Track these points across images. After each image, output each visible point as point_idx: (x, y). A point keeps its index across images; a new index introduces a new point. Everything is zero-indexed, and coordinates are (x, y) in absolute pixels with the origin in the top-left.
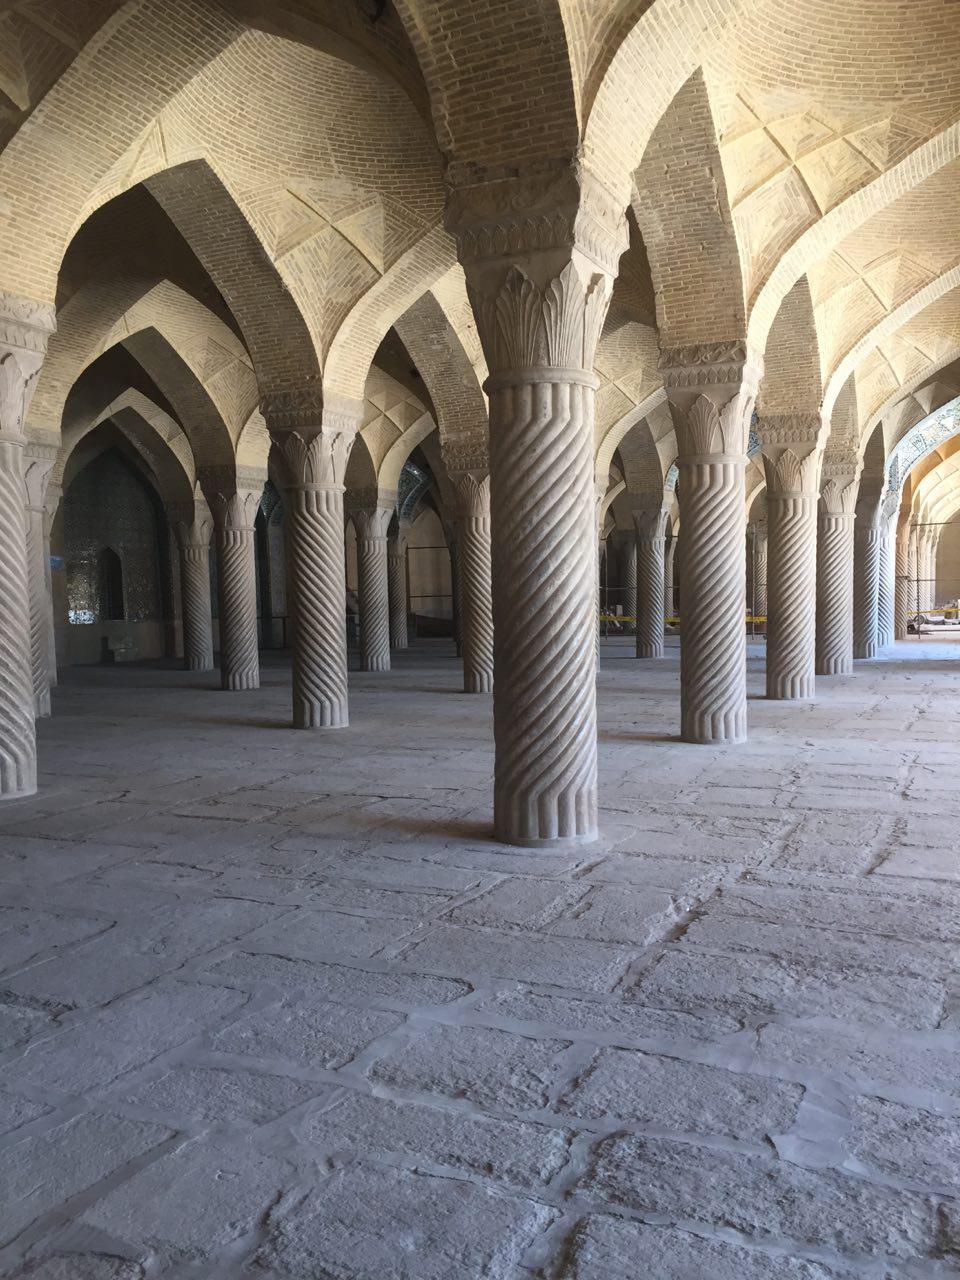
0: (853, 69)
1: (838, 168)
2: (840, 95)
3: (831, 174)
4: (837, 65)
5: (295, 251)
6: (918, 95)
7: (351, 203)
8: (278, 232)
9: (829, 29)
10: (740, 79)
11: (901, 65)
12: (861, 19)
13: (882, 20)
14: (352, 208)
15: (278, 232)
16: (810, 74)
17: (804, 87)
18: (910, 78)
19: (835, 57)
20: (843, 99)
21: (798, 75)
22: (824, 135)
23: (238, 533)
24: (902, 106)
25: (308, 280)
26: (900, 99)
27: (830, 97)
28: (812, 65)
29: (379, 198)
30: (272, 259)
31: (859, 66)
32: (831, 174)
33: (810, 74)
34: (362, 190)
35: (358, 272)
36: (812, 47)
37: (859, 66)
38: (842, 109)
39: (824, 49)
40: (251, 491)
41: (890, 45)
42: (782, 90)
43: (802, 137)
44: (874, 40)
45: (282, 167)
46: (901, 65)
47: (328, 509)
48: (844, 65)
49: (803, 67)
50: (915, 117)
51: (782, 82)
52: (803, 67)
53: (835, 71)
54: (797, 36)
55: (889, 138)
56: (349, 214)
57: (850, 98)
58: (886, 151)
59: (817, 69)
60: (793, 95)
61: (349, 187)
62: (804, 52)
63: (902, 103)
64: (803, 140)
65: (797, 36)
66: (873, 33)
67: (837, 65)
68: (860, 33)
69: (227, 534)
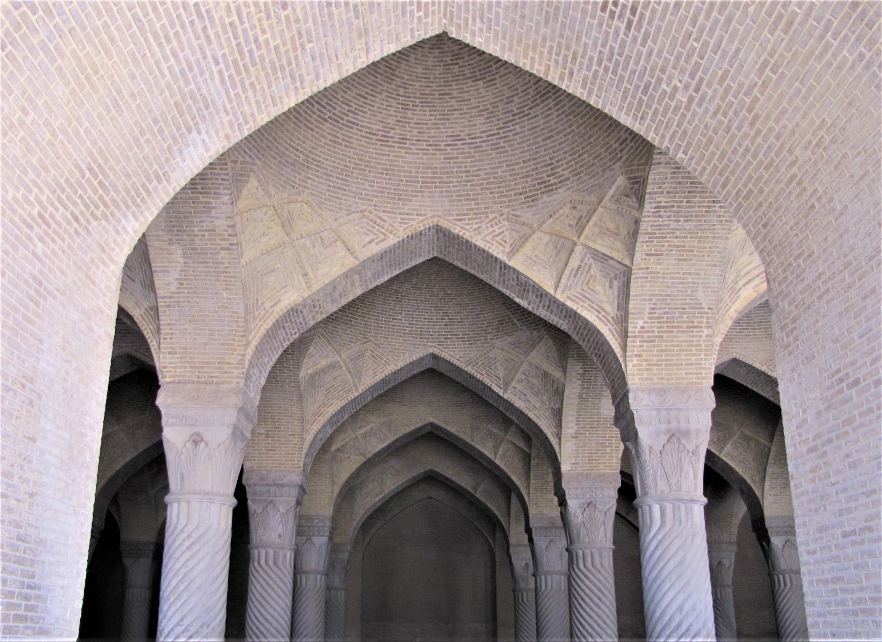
0: (586, 156)
1: (618, 227)
2: (586, 178)
3: (616, 234)
4: (574, 159)
5: (514, 384)
6: (629, 147)
7: (531, 342)
8: (501, 375)
9: (553, 142)
10: (505, 211)
11: (610, 134)
12: (567, 122)
13: (578, 114)
14: (533, 347)
15: (501, 375)
16: (561, 176)
17: (560, 187)
18: (619, 139)
19: (570, 155)
20: (590, 179)
21: (553, 181)
22: (589, 212)
23: (781, 576)
24: (624, 162)
25: (534, 400)
26: (621, 157)
27: (581, 183)
28: (559, 170)
29: (545, 332)
30: (501, 394)
31: (587, 151)
32: (616, 234)
33: (561, 176)
34: (535, 332)
35: (555, 385)
36: (551, 159)
37: (587, 151)
38: (592, 186)
39: (560, 155)
40: (788, 537)
41: (595, 126)
42: (546, 198)
43: (575, 221)
44: (585, 128)
45: (489, 336)
46: (610, 134)
47: (584, 565)
48: (579, 156)
49: (553, 174)
50: (634, 165)
51: (543, 193)
52: (553, 174)
53: (576, 164)
54: (535, 159)
55: (632, 189)
56: (532, 350)
57: (594, 176)
58: (635, 200)
59: (563, 170)
60: (555, 197)
61: (528, 333)
62: (547, 166)
63: (624, 159)
64: (577, 223)
65: (535, 159)
66: (581, 125)
67: (574, 159)
68: (573, 131)
69: (778, 578)
